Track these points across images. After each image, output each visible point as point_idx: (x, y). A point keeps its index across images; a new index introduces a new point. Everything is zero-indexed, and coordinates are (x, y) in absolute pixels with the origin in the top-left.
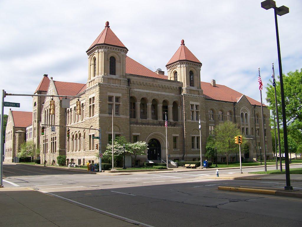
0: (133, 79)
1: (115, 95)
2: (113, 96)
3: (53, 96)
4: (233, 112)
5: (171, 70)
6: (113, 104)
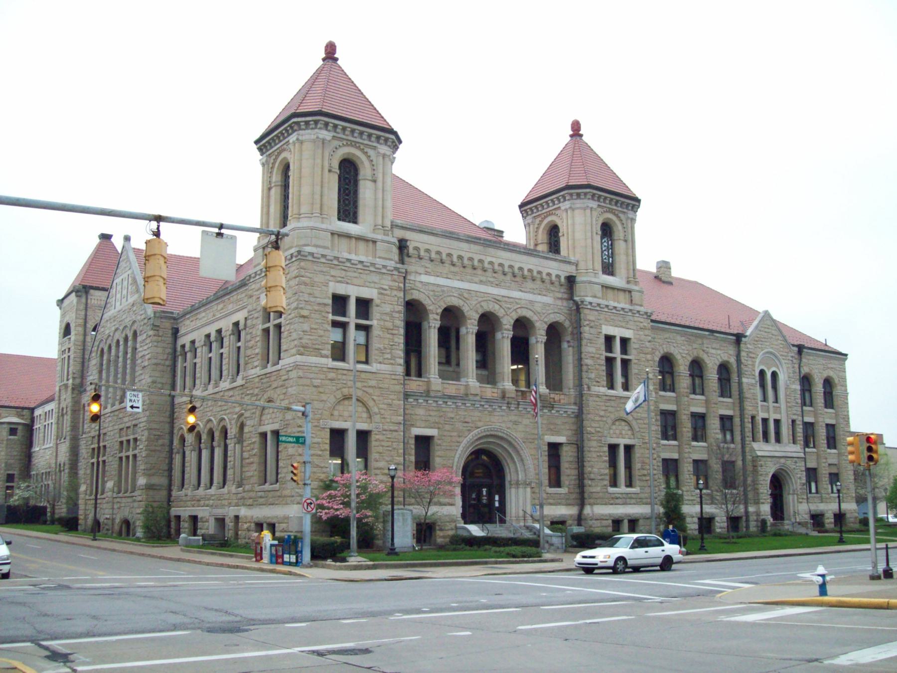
0: (415, 240)
1: (353, 292)
2: (349, 296)
3: (159, 219)
4: (735, 366)
5: (537, 221)
6: (348, 323)
